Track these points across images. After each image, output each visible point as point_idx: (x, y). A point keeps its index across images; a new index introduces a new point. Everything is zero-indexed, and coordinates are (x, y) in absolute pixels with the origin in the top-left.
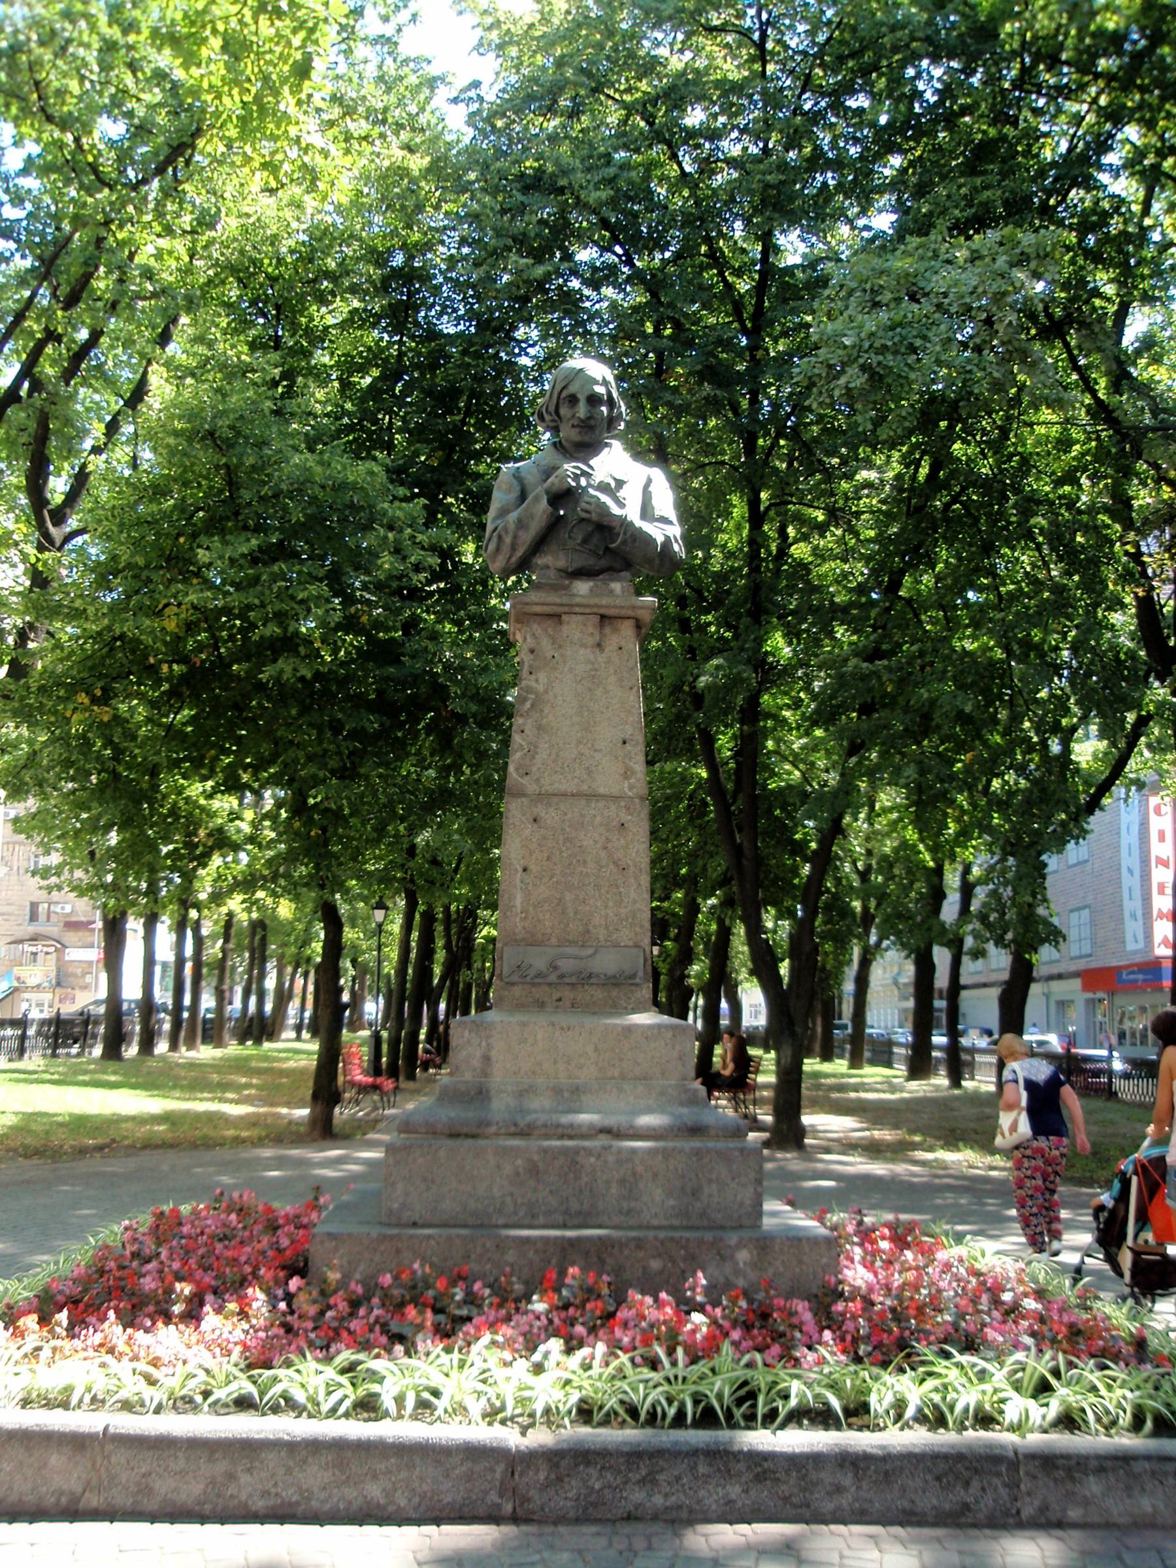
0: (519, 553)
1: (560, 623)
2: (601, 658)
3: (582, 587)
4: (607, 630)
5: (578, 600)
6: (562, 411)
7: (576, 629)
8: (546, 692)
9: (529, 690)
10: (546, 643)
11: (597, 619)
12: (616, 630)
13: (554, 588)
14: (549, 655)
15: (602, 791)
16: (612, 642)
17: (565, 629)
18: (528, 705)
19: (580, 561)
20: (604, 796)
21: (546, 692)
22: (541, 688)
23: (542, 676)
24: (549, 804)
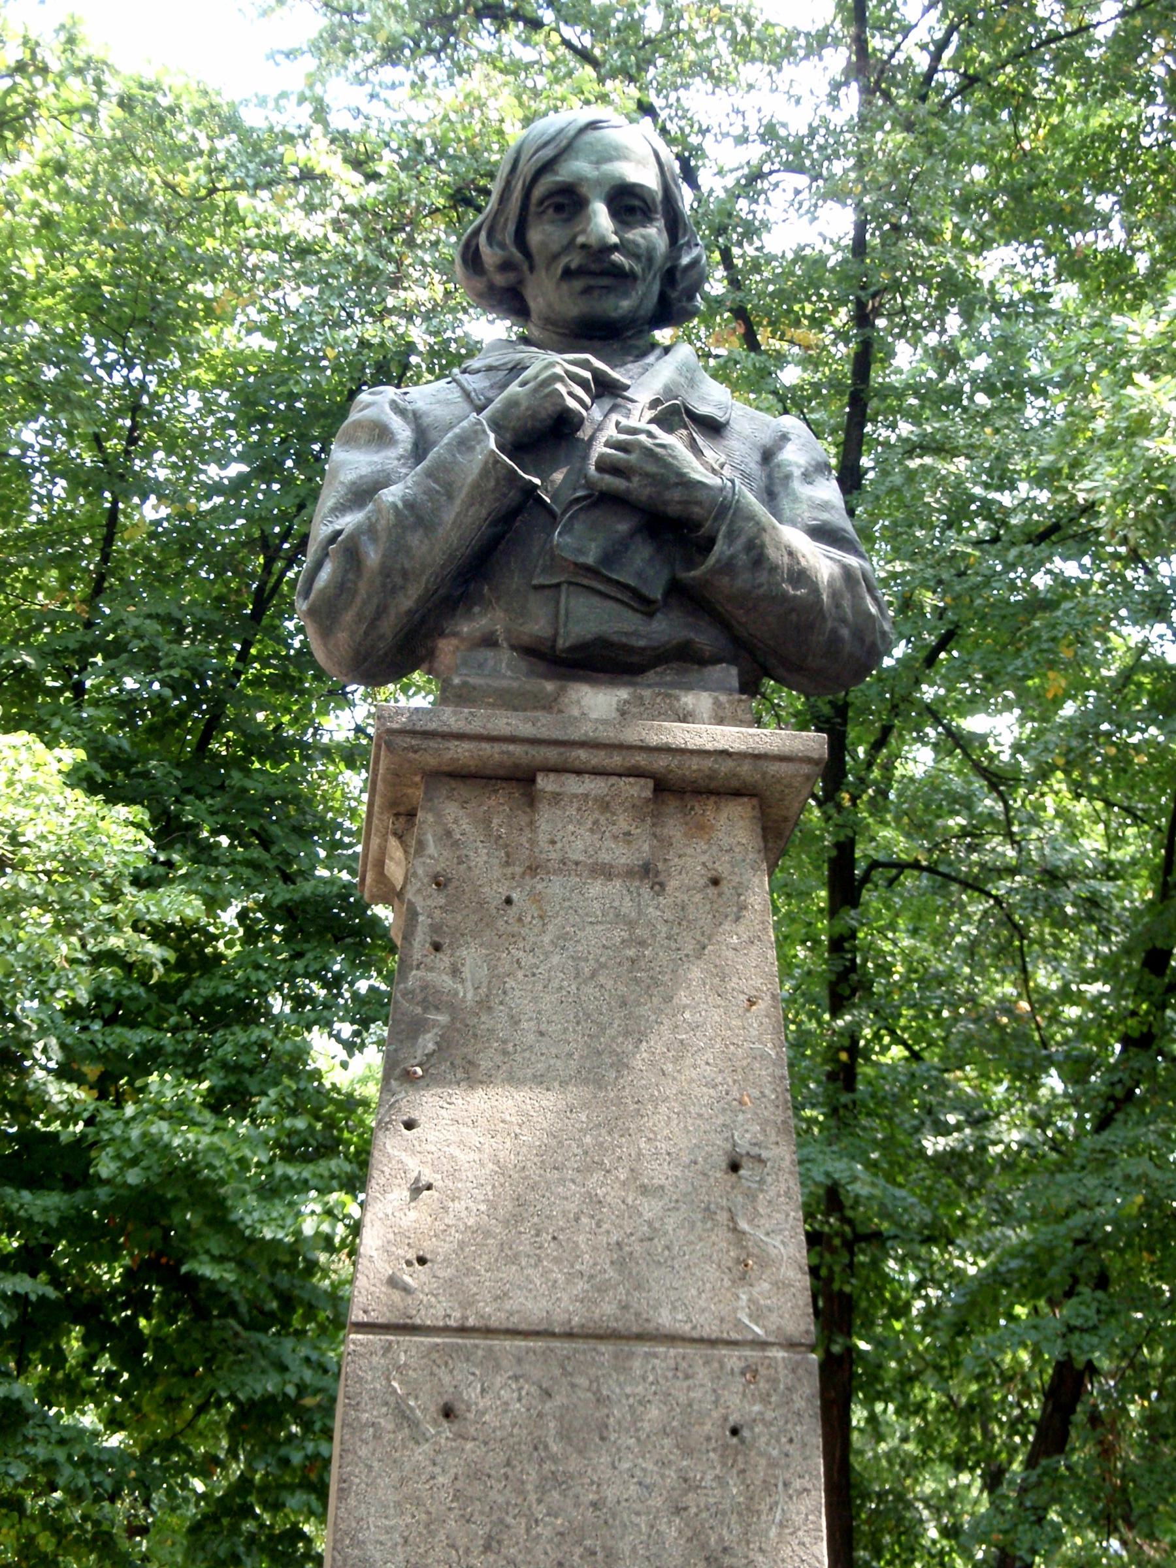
0: (407, 601)
1: (531, 799)
2: (655, 910)
3: (596, 704)
4: (674, 828)
5: (585, 730)
6: (535, 237)
7: (575, 827)
8: (484, 1005)
9: (431, 999)
10: (482, 858)
11: (639, 790)
12: (702, 829)
13: (509, 701)
14: (494, 892)
15: (665, 1319)
16: (690, 861)
17: (546, 819)
18: (428, 1042)
19: (589, 618)
20: (672, 1339)
21: (484, 1005)
22: (467, 995)
23: (471, 956)
24: (493, 1362)
